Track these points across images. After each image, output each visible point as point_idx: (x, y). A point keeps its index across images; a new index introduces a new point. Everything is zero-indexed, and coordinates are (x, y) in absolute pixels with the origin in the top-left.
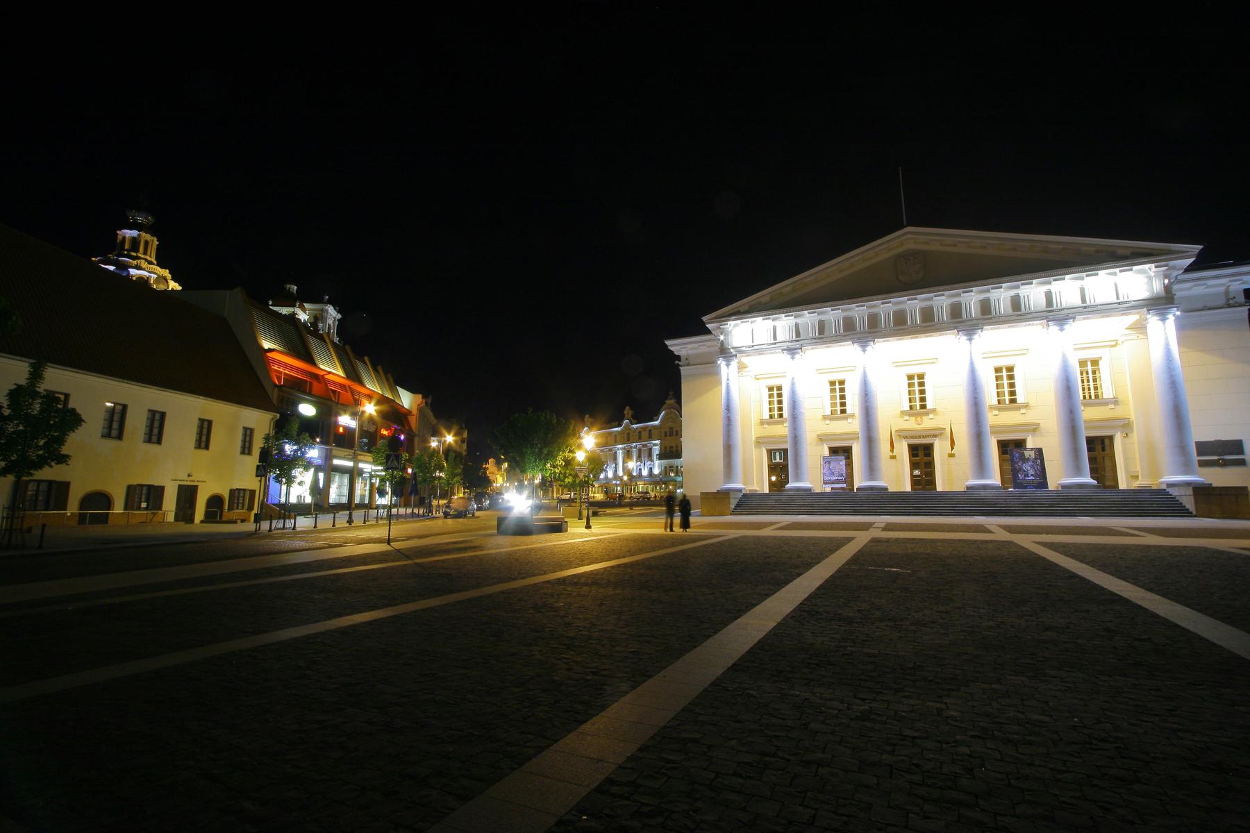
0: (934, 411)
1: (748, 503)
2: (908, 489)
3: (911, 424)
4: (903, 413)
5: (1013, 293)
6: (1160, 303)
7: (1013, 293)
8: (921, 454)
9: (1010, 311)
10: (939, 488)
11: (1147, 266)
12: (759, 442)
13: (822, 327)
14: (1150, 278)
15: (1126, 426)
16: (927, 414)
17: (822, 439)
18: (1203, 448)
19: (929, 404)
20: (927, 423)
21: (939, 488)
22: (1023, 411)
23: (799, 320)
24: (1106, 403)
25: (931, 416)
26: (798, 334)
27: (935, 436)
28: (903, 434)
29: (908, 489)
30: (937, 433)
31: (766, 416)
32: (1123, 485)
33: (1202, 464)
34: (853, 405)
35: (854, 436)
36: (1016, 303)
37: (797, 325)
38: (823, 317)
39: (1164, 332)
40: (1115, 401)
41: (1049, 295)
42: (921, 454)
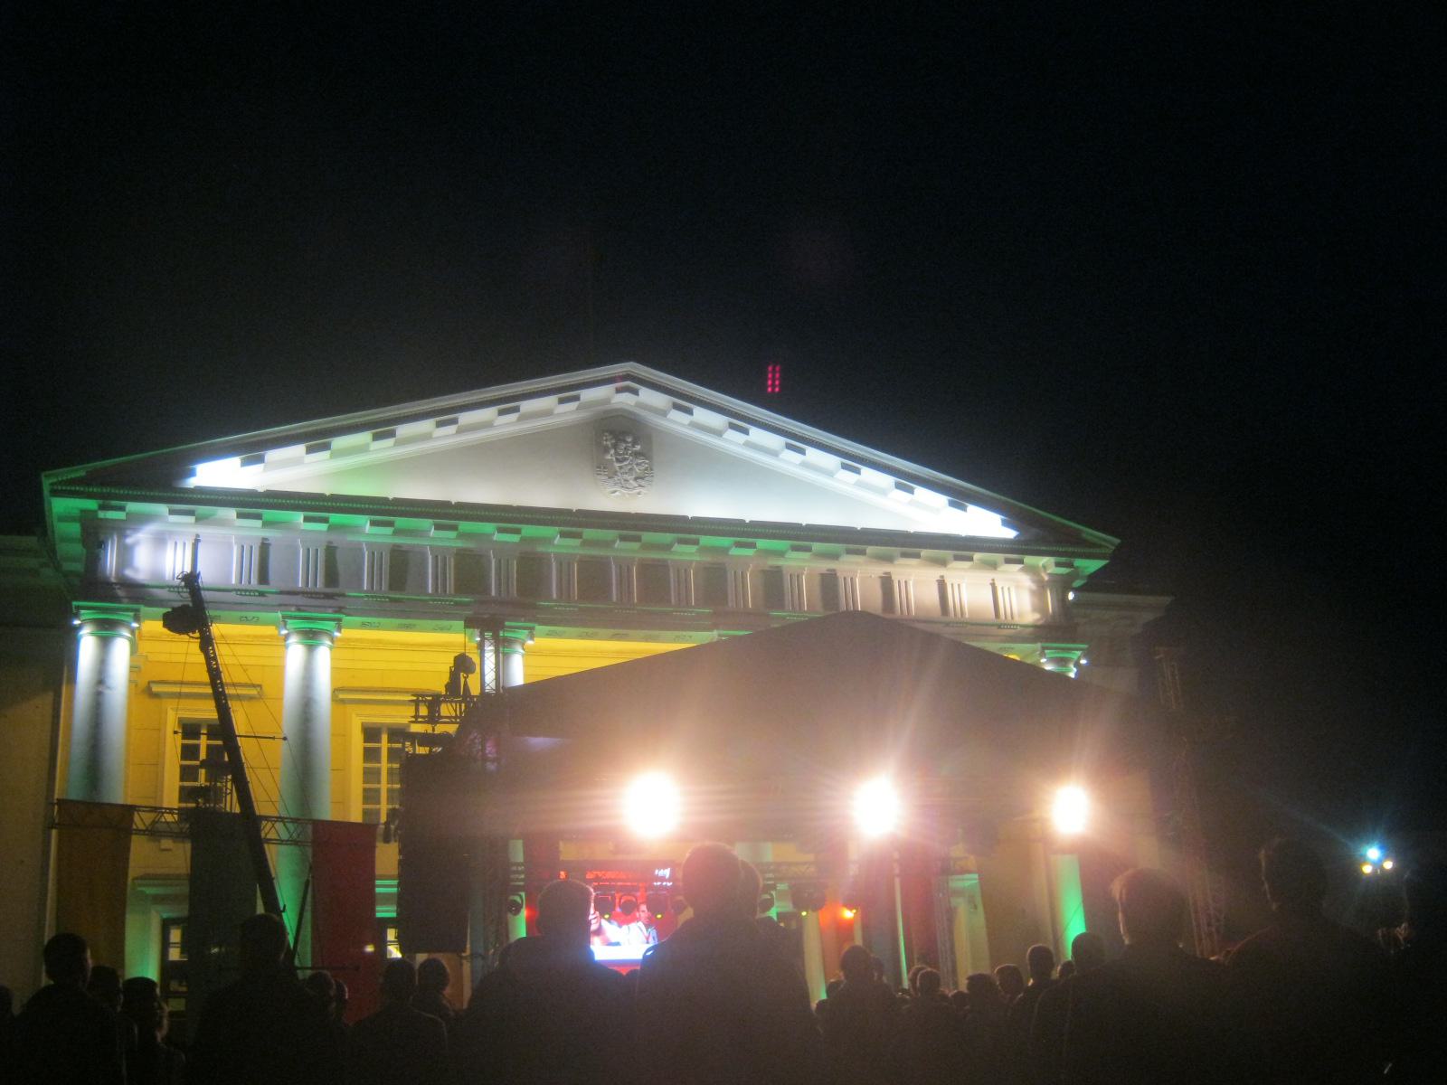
5: (825, 566)
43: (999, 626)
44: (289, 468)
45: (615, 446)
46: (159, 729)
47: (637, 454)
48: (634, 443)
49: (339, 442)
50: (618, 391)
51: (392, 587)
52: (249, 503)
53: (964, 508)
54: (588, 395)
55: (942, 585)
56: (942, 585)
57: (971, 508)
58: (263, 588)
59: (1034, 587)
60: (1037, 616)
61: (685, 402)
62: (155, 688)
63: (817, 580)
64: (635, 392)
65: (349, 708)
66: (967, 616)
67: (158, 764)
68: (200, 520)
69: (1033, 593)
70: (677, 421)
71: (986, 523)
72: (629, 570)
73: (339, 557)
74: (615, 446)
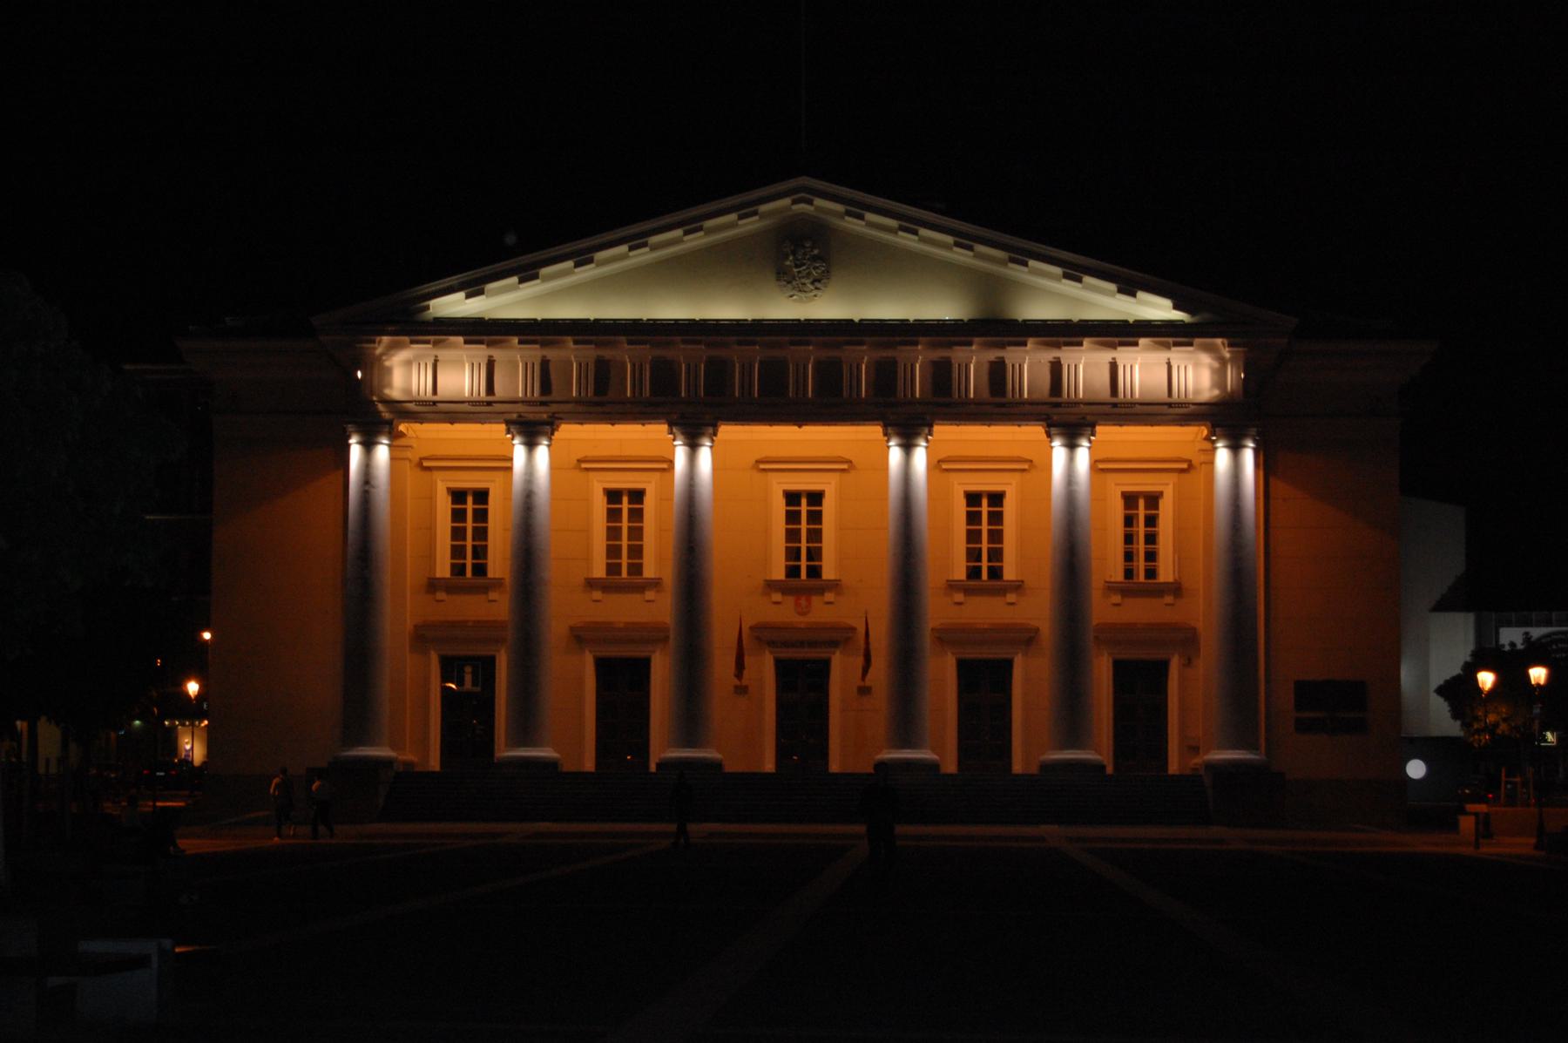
0: (835, 586)
1: (407, 791)
2: (769, 766)
3: (783, 611)
4: (771, 586)
5: (993, 355)
6: (1224, 418)
7: (993, 355)
8: (803, 683)
9: (986, 394)
10: (834, 767)
11: (1219, 341)
12: (423, 637)
13: (603, 375)
14: (1223, 362)
15: (1187, 640)
16: (821, 591)
17: (580, 637)
18: (1307, 693)
19: (828, 573)
20: (822, 611)
21: (834, 767)
22: (1011, 597)
23: (552, 354)
24: (1159, 591)
25: (829, 596)
26: (546, 386)
27: (834, 644)
28: (767, 635)
29: (769, 766)
30: (839, 637)
31: (443, 570)
32: (1173, 767)
33: (1302, 726)
34: (658, 559)
35: (653, 635)
36: (997, 372)
37: (545, 364)
38: (607, 353)
39: (1234, 467)
40: (1176, 589)
41: (1056, 367)
42: (803, 683)
43: (1170, 405)
44: (505, 300)
45: (794, 253)
46: (431, 498)
47: (815, 258)
48: (812, 248)
49: (544, 271)
50: (795, 202)
51: (596, 393)
52: (477, 330)
53: (1134, 295)
54: (764, 208)
55: (1114, 367)
56: (1114, 367)
57: (1140, 294)
58: (490, 398)
59: (1216, 365)
60: (1216, 392)
61: (857, 209)
62: (426, 464)
63: (986, 368)
64: (810, 202)
65: (591, 474)
66: (1137, 395)
67: (431, 529)
68: (436, 344)
69: (1214, 371)
70: (853, 225)
71: (1157, 308)
72: (805, 368)
73: (552, 367)
74: (794, 253)
